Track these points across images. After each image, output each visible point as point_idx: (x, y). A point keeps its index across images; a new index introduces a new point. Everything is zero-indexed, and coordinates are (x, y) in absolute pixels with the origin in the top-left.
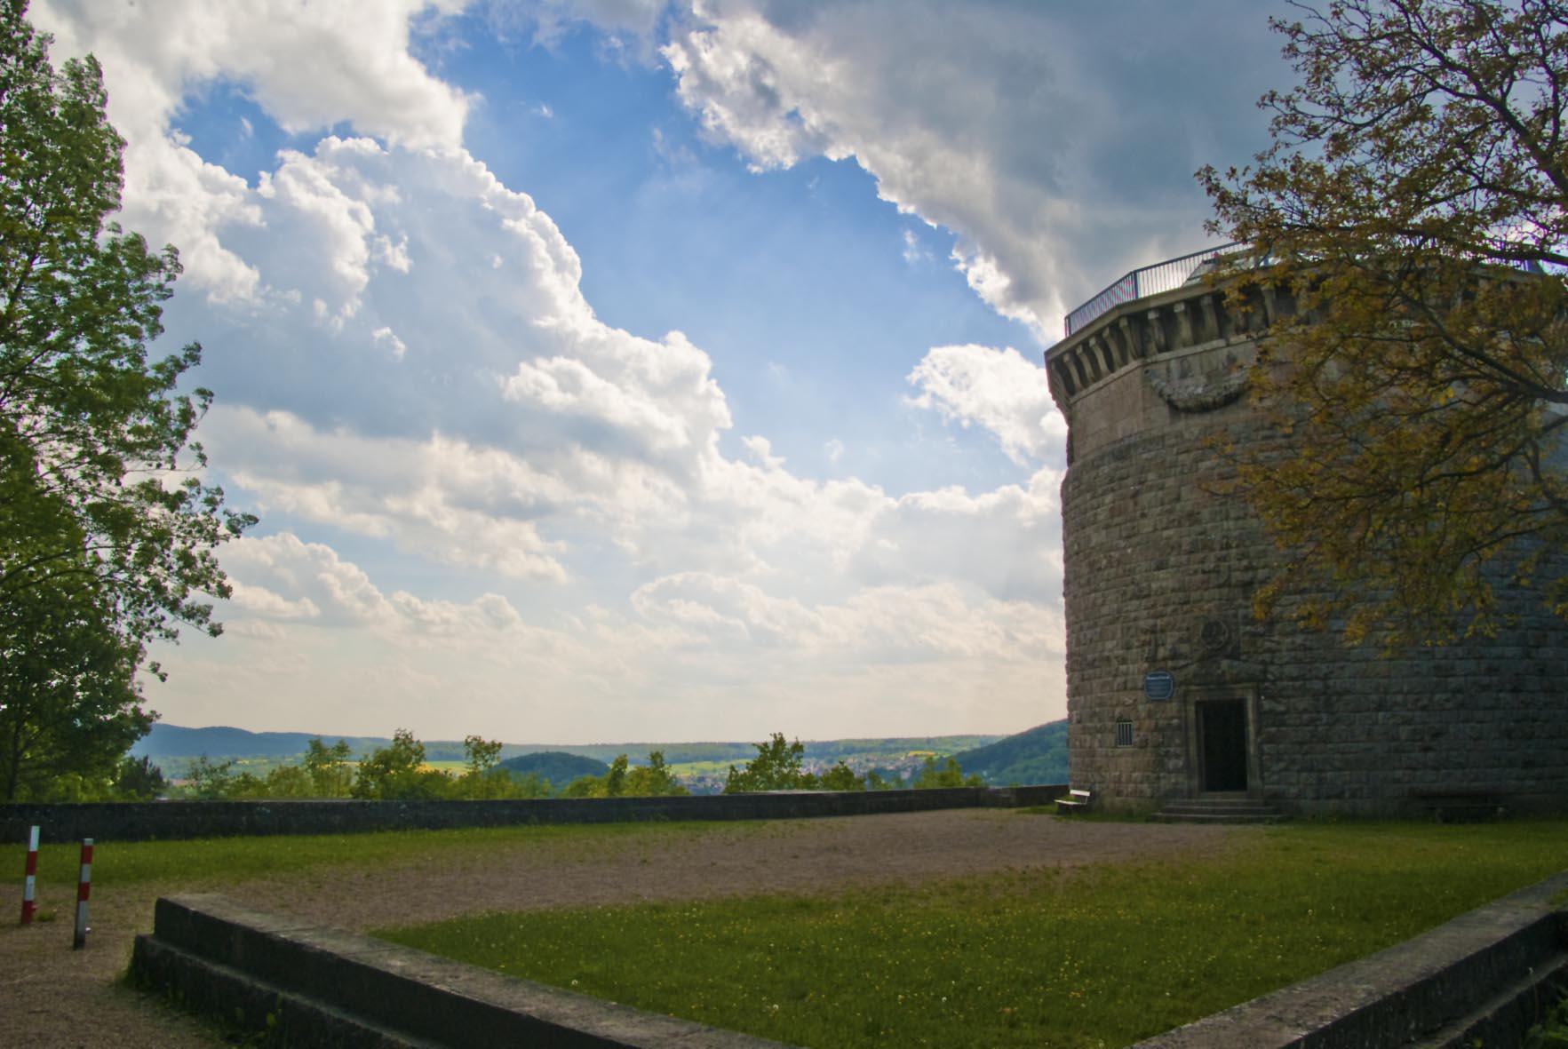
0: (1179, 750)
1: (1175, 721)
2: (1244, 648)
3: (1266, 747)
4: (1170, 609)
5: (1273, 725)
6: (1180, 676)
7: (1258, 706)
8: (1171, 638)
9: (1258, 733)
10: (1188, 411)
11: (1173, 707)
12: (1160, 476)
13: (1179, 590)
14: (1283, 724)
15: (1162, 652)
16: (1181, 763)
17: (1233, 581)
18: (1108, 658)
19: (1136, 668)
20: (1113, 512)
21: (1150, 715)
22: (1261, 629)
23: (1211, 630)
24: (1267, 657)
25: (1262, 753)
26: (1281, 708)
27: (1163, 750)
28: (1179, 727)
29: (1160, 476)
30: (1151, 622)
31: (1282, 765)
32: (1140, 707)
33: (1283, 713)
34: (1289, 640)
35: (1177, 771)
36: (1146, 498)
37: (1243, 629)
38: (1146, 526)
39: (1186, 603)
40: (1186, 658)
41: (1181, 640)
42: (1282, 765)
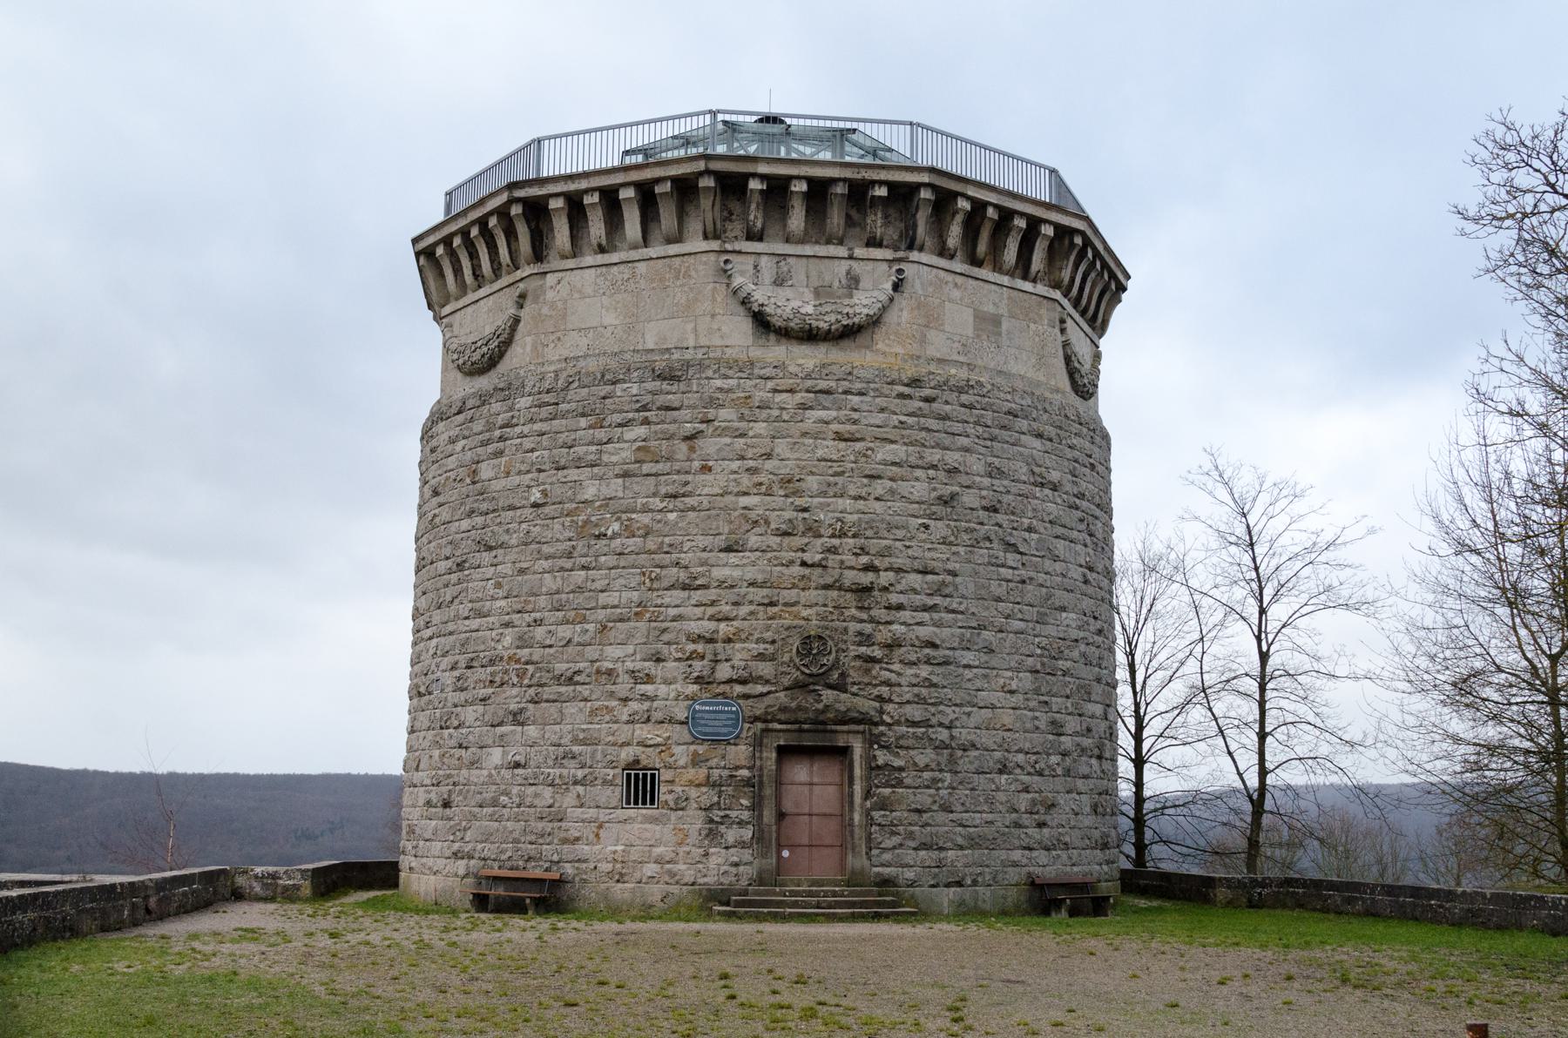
0: (745, 815)
1: (745, 773)
2: (854, 675)
3: (876, 814)
4: (744, 610)
5: (886, 786)
6: (759, 708)
7: (869, 758)
8: (740, 654)
9: (867, 794)
10: (785, 333)
11: (740, 753)
12: (742, 418)
13: (763, 585)
14: (900, 783)
15: (724, 672)
16: (747, 833)
17: (847, 583)
18: (610, 672)
19: (671, 690)
20: (644, 452)
21: (696, 761)
22: (877, 652)
23: (810, 645)
24: (884, 691)
25: (871, 822)
26: (898, 763)
27: (717, 815)
28: (748, 783)
29: (742, 418)
30: (712, 625)
31: (896, 840)
32: (677, 750)
33: (901, 769)
34: (910, 671)
35: (742, 844)
36: (710, 445)
37: (854, 650)
38: (709, 485)
39: (772, 604)
40: (767, 682)
41: (761, 657)
42: (896, 840)
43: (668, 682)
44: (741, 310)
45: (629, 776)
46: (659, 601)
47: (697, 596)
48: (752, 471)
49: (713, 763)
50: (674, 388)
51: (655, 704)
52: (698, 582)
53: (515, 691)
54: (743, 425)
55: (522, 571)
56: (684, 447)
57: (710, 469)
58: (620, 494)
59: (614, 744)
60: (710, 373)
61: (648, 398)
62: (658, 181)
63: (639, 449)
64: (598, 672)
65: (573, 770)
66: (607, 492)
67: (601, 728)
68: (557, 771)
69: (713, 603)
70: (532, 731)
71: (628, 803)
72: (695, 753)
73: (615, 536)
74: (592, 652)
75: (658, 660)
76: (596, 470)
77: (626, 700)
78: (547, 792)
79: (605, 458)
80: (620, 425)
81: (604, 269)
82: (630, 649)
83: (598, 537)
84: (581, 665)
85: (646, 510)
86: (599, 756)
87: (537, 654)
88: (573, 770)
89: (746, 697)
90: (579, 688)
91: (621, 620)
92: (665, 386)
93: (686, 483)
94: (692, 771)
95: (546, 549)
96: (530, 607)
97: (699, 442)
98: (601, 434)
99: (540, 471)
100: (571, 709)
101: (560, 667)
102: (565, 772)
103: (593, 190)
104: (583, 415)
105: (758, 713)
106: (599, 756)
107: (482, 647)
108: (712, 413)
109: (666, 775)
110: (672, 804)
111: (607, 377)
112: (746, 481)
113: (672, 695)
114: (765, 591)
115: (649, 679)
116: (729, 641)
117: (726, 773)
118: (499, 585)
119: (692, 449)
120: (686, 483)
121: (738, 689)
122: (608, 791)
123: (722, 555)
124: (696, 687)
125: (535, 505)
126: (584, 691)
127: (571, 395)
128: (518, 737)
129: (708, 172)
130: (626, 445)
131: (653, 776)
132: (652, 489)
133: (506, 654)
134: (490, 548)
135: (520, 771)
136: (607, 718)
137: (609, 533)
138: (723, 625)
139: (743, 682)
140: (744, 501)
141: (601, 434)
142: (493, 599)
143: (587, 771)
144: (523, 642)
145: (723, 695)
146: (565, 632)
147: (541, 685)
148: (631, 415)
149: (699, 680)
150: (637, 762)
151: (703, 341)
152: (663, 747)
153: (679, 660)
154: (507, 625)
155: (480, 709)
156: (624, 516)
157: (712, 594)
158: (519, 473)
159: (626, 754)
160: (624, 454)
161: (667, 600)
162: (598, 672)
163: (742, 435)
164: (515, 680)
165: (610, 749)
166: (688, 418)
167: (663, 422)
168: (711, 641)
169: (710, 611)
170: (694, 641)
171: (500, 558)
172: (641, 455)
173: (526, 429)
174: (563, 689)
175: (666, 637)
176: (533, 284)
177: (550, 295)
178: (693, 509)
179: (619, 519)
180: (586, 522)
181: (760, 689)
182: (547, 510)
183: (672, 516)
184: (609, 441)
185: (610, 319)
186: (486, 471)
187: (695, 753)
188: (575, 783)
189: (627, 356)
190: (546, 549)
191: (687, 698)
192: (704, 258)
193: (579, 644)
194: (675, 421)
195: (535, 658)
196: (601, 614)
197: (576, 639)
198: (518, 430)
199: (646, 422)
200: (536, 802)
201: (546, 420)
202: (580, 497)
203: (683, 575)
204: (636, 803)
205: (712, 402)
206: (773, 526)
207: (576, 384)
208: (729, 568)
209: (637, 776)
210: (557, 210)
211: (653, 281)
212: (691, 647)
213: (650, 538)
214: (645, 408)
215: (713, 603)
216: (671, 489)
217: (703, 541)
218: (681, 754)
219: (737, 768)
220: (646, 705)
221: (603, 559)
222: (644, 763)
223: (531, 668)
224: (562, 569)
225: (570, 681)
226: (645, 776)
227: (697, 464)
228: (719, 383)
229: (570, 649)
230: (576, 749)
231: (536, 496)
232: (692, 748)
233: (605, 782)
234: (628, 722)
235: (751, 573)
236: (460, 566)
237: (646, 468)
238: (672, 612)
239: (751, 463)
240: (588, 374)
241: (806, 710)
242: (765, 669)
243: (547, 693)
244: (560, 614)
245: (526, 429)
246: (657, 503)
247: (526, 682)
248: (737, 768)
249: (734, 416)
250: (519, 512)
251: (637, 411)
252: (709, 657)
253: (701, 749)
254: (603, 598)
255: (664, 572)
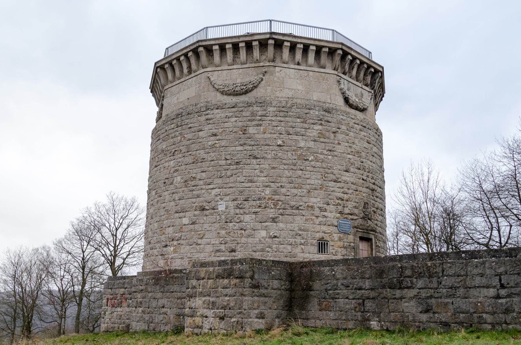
4: (350, 191)
10: (351, 106)
12: (347, 130)
15: (347, 211)
18: (312, 207)
19: (332, 215)
20: (321, 134)
21: (340, 239)
29: (347, 130)
30: (343, 195)
36: (340, 136)
38: (340, 149)
39: (357, 191)
41: (355, 207)
43: (331, 212)
44: (341, 95)
45: (319, 243)
46: (328, 185)
47: (339, 185)
48: (350, 147)
49: (345, 240)
50: (329, 115)
51: (328, 219)
52: (339, 180)
53: (272, 210)
54: (348, 132)
55: (274, 168)
56: (332, 135)
57: (340, 144)
58: (313, 147)
59: (314, 232)
60: (339, 113)
61: (322, 117)
62: (324, 47)
63: (319, 133)
64: (308, 206)
65: (299, 240)
66: (309, 146)
67: (309, 226)
68: (294, 240)
69: (343, 188)
70: (281, 225)
71: (319, 252)
72: (340, 237)
73: (312, 161)
74: (304, 199)
75: (328, 204)
76: (304, 137)
77: (317, 217)
78: (289, 247)
79: (308, 134)
80: (313, 124)
81: (229, 71)
82: (319, 200)
83: (306, 160)
84: (301, 204)
85: (322, 154)
86: (309, 236)
87: (283, 198)
88: (299, 240)
89: (352, 219)
90: (301, 211)
91: (315, 189)
92: (326, 114)
93: (334, 147)
94: (339, 242)
95: (284, 161)
96: (278, 181)
97: (337, 135)
98: (306, 126)
99: (281, 134)
100: (298, 218)
101: (293, 203)
102: (297, 240)
103: (301, 43)
104: (298, 118)
105: (356, 225)
106: (309, 236)
107: (254, 193)
108: (340, 126)
109: (331, 243)
110: (334, 253)
111: (307, 107)
112: (349, 150)
113: (332, 217)
114: (355, 186)
115: (325, 210)
116: (347, 201)
117: (348, 244)
118: (261, 172)
119: (335, 136)
120: (334, 147)
121: (350, 217)
122: (313, 248)
123: (345, 172)
124: (339, 215)
125: (280, 146)
126: (303, 212)
127: (293, 110)
128: (275, 227)
129: (342, 49)
130: (315, 131)
131: (327, 243)
132: (324, 147)
133: (267, 197)
134: (257, 158)
135: (276, 239)
136: (312, 222)
137: (310, 159)
138: (345, 195)
139: (351, 214)
140: (349, 156)
141: (306, 126)
142: (258, 176)
143: (305, 240)
144: (275, 193)
145: (346, 218)
146: (295, 191)
147: (285, 209)
148: (317, 121)
149: (341, 213)
150: (323, 238)
151: (333, 102)
152: (330, 234)
153: (333, 205)
154: (267, 186)
155: (254, 216)
156: (315, 154)
157: (342, 185)
158: (271, 133)
159: (319, 235)
160: (315, 134)
161: (330, 185)
162: (308, 206)
163: (348, 135)
164: (273, 206)
165: (313, 233)
166: (334, 126)
167: (326, 126)
168: (343, 200)
169: (342, 190)
170: (338, 199)
171: (262, 162)
172: (320, 135)
173: (273, 119)
174: (294, 211)
175: (330, 197)
176: (272, 69)
177: (277, 74)
178: (336, 156)
179: (313, 155)
180: (301, 154)
181: (355, 217)
182: (284, 148)
183: (330, 157)
184: (309, 128)
185: (300, 87)
186: (251, 130)
187: (340, 237)
188: (301, 244)
189: (312, 101)
190: (284, 161)
191: (337, 218)
192: (333, 76)
193: (300, 196)
194: (330, 126)
195: (281, 199)
196: (308, 187)
197: (299, 194)
198: (269, 118)
199: (321, 124)
200: (284, 250)
201: (283, 117)
202: (298, 146)
203: (334, 178)
204: (322, 252)
205: (340, 123)
206: (356, 166)
207: (295, 107)
208: (347, 177)
209: (322, 243)
210: (242, 47)
211: (315, 79)
212: (337, 201)
213: (323, 163)
214: (321, 120)
215: (343, 188)
216: (330, 148)
217: (339, 167)
218: (336, 236)
219: (351, 242)
220: (325, 219)
221: (308, 168)
222: (325, 239)
223: (280, 203)
224: (292, 169)
225: (297, 208)
226: (324, 243)
227: (336, 142)
228: (342, 117)
229: (297, 197)
230: (300, 232)
231: (280, 142)
232: (339, 235)
233: (312, 245)
234: (319, 224)
235: (352, 180)
236: (238, 163)
237: (322, 140)
238: (332, 189)
239: (350, 145)
240: (300, 104)
241: (364, 225)
242: (356, 211)
243: (289, 211)
244: (292, 185)
245: (273, 119)
246: (325, 152)
247: (278, 207)
248: (351, 242)
249: (345, 129)
250: (271, 147)
251: (318, 120)
252: (342, 205)
253: (341, 235)
254: (308, 181)
255: (328, 175)
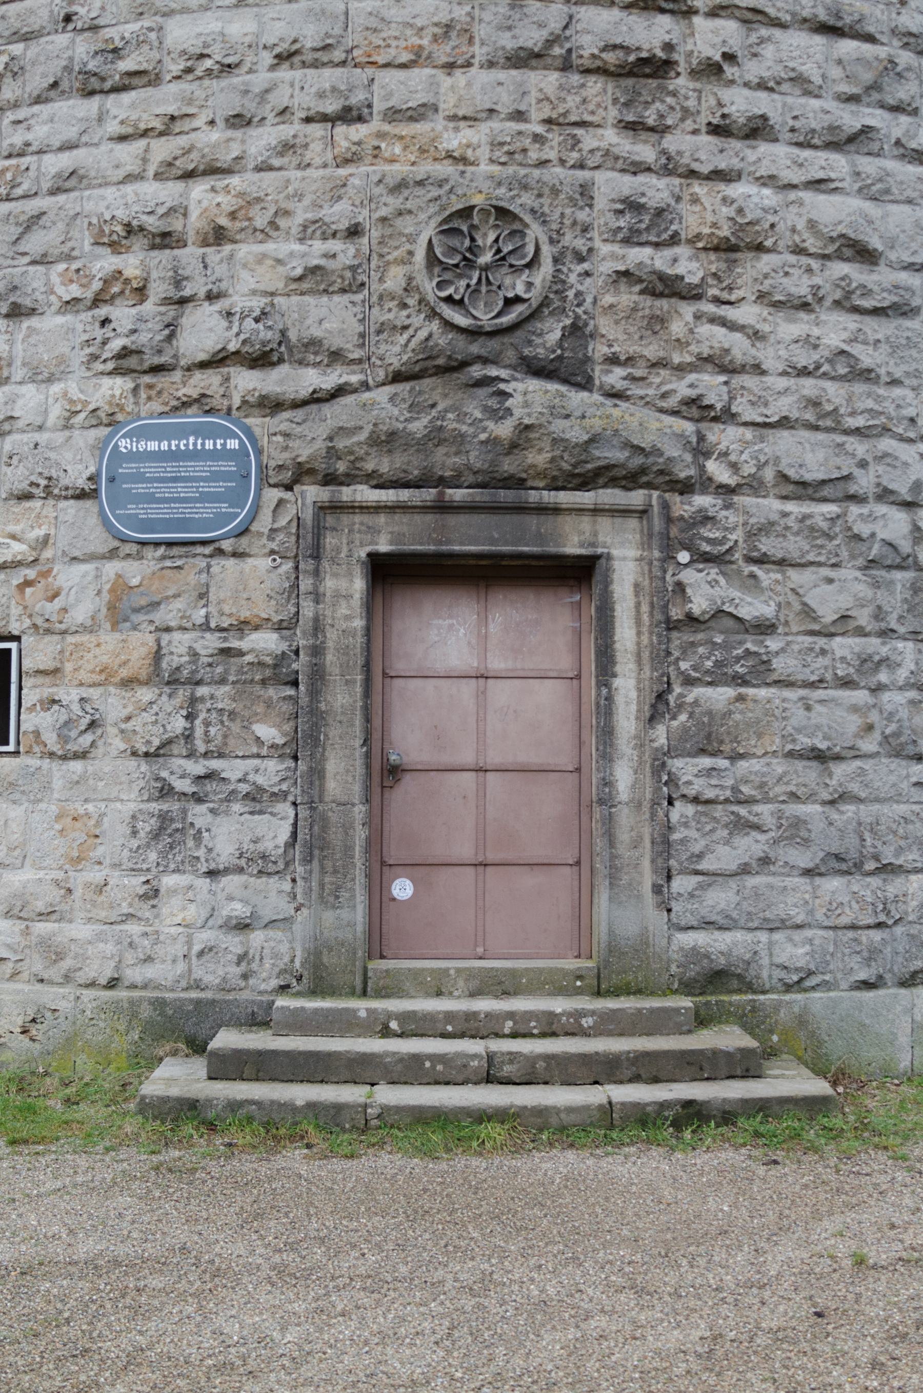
0: (270, 773)
1: (266, 642)
2: (612, 334)
3: (687, 768)
4: (261, 141)
5: (718, 677)
6: (309, 437)
7: (665, 596)
8: (252, 274)
9: (658, 706)
11: (252, 581)
13: (320, 56)
14: (761, 671)
15: (203, 332)
16: (274, 829)
17: (588, 45)
21: (120, 610)
22: (688, 266)
23: (473, 239)
24: (711, 386)
25: (669, 792)
26: (752, 608)
27: (182, 771)
28: (279, 672)
30: (168, 192)
31: (750, 846)
32: (69, 577)
33: (764, 628)
34: (790, 328)
35: (256, 863)
37: (611, 257)
39: (350, 115)
40: (336, 356)
41: (314, 279)
42: (750, 846)
43: (42, 376)
46: (18, 138)
47: (123, 108)
49: (168, 614)
52: (127, 65)
72: (120, 588)
89: (272, 405)
94: (109, 639)
105: (304, 453)
110: (51, 739)
113: (56, 412)
114: (328, 77)
116: (218, 236)
117: (210, 643)
121: (247, 382)
124: (120, 385)
138: (199, 190)
139: (262, 360)
149: (126, 361)
153: (71, 304)
157: (165, 99)
161: (39, 133)
168: (165, 240)
169: (162, 149)
170: (115, 246)
175: (36, 243)
187: (120, 588)
203: (82, 49)
218: (81, 589)
219: (243, 627)
232: (111, 568)
242: (330, 318)
248: (243, 627)
252: (158, 289)
253: (135, 572)
255: (34, 49)
